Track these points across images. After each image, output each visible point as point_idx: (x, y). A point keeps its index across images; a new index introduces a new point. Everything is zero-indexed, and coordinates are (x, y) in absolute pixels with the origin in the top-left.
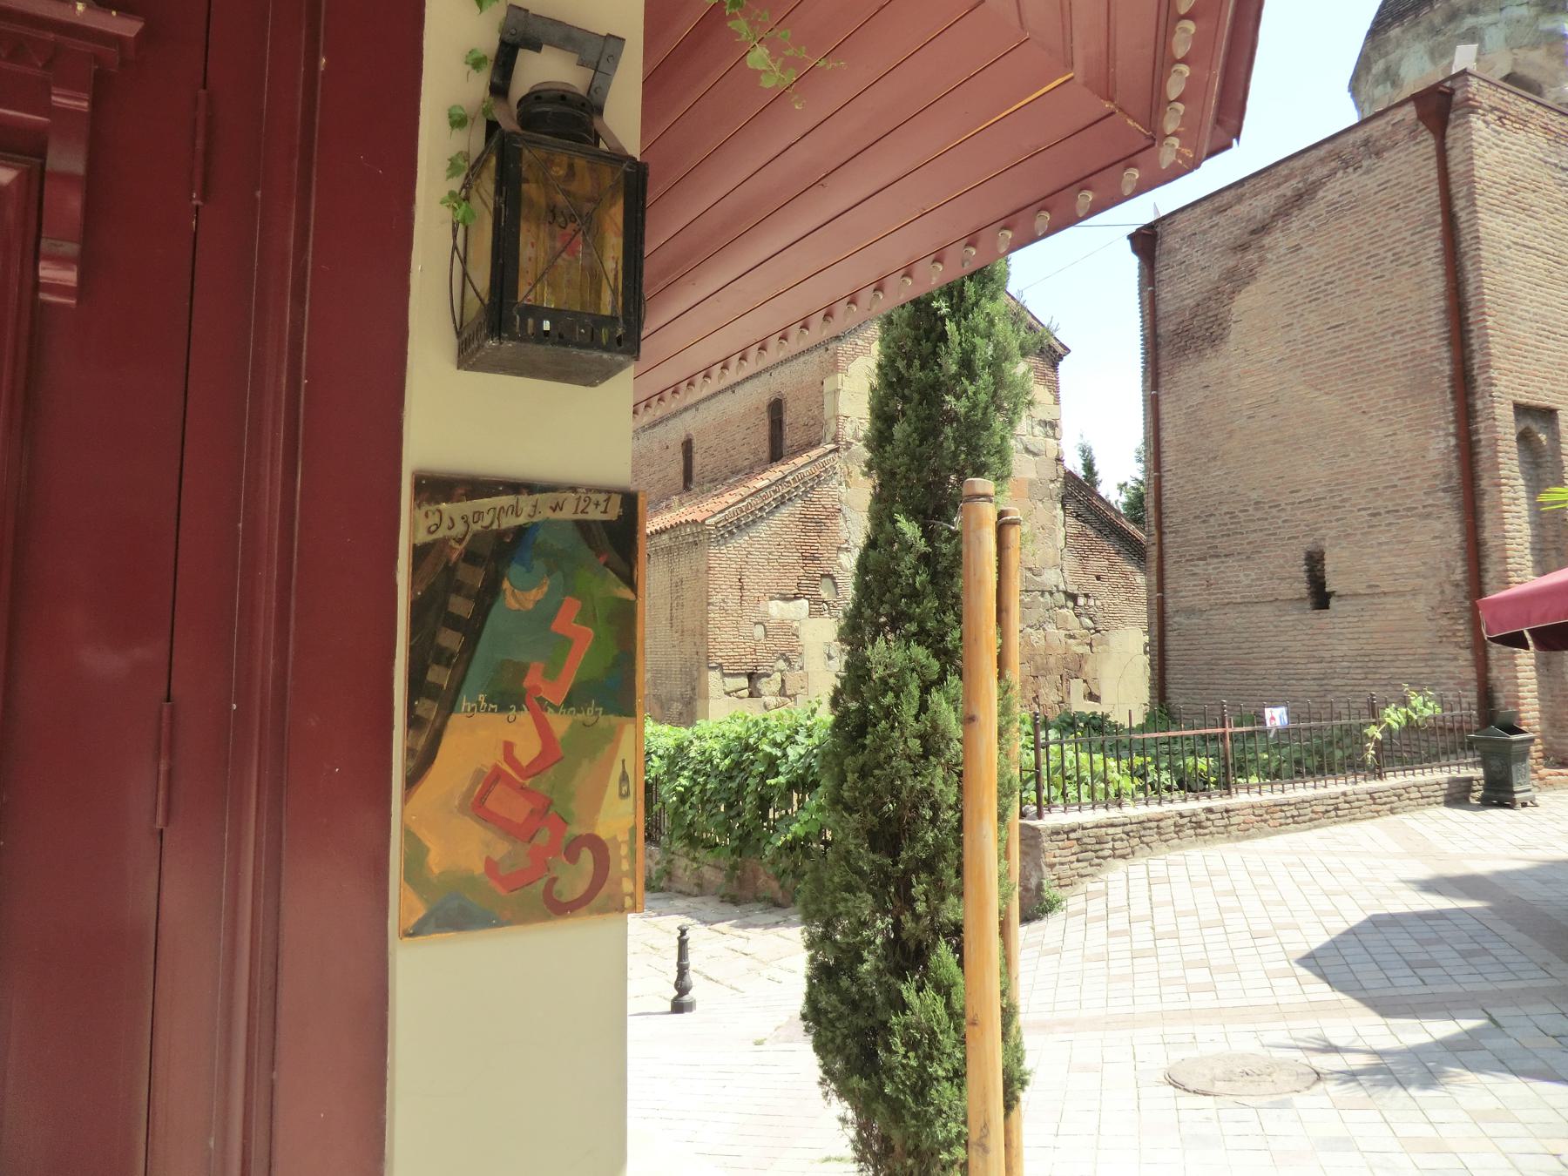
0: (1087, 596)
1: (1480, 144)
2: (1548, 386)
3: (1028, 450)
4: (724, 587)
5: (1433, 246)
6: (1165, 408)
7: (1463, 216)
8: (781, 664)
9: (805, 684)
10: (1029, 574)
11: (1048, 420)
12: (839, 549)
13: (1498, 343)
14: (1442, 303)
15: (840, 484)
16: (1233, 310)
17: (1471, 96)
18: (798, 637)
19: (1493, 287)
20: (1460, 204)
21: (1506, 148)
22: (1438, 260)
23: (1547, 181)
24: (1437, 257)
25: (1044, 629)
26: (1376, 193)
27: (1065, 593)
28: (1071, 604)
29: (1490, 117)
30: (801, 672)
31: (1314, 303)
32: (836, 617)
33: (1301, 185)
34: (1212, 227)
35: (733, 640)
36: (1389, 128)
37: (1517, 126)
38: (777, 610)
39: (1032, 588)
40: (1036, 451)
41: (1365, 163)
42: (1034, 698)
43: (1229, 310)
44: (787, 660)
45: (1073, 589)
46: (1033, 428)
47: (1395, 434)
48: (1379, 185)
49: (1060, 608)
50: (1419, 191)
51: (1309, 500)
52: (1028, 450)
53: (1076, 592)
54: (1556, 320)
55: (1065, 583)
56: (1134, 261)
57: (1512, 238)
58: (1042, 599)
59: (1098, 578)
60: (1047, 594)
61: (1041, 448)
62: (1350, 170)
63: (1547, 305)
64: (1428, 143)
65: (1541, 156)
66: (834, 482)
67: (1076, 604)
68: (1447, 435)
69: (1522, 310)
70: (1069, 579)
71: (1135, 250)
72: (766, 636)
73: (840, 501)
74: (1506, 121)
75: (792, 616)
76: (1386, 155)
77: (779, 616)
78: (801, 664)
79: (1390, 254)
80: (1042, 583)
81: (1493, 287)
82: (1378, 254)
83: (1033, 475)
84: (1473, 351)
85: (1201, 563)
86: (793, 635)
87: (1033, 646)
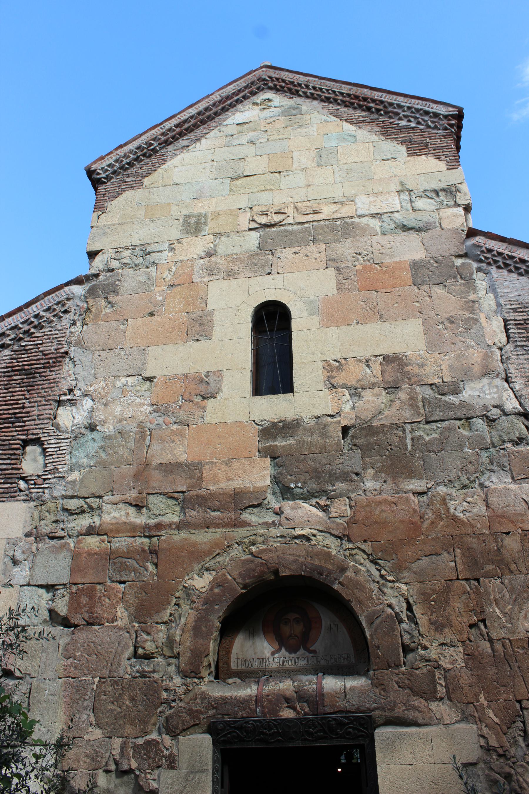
11: (438, 186)
12: (59, 403)
15: (74, 324)
25: (482, 485)
39: (438, 415)
40: (421, 225)
58: (466, 433)
73: (69, 343)
80: (463, 404)
83: (420, 255)
87: (455, 519)
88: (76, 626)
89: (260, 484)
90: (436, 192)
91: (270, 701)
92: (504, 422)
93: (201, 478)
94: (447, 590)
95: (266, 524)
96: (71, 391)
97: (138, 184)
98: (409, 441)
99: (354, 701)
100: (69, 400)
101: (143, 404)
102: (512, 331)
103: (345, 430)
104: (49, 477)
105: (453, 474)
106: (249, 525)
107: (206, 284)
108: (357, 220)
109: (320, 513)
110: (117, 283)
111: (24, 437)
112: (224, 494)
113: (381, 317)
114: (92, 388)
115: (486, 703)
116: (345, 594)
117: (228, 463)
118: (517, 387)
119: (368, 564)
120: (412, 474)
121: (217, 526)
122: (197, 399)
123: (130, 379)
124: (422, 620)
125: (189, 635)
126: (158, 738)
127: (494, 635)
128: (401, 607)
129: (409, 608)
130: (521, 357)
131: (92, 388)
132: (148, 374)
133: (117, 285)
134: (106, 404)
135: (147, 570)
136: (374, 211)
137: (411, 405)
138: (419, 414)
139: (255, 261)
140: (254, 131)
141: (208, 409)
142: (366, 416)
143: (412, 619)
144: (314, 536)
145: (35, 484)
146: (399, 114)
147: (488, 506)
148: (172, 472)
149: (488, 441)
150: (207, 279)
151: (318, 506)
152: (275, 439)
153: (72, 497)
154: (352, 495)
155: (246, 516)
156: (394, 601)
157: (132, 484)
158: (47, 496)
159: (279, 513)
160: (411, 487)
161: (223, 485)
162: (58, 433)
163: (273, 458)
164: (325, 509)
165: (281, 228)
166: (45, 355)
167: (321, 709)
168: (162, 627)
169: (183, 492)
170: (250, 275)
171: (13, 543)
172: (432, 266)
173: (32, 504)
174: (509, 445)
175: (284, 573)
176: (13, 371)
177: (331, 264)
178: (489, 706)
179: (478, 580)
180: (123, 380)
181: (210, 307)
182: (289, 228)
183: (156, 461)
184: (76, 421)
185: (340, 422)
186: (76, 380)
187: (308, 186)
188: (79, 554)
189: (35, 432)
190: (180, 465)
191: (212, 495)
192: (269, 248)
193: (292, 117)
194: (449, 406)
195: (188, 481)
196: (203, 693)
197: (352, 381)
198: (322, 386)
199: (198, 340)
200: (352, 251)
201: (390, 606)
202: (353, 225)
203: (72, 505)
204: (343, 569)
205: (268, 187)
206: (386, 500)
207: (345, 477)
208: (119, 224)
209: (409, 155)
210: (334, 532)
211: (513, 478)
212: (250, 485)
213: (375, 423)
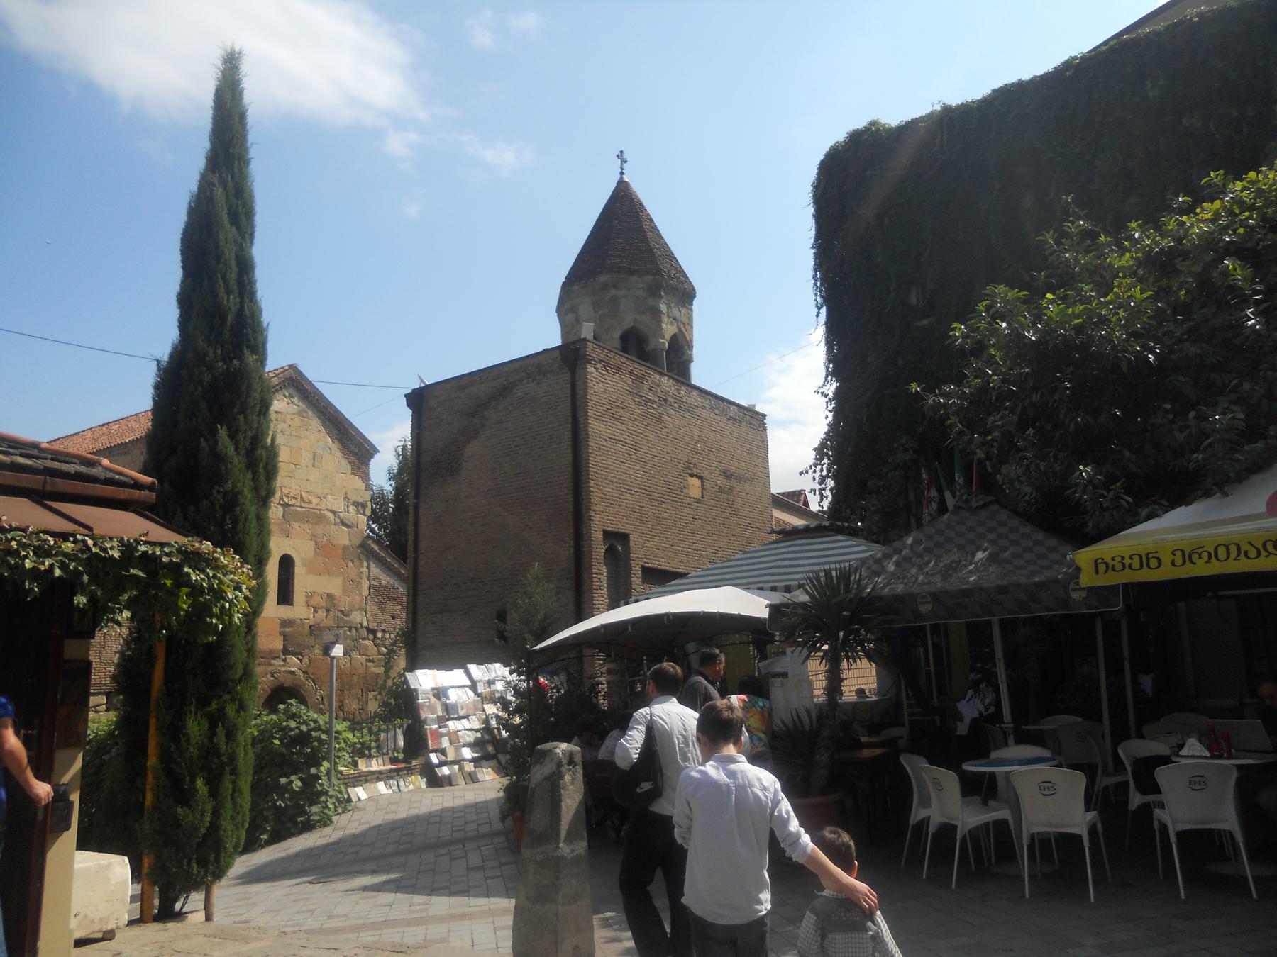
0: (384, 631)
1: (592, 381)
2: (625, 520)
5: (568, 435)
6: (422, 512)
7: (581, 419)
10: (340, 615)
11: (360, 501)
13: (596, 496)
14: (570, 469)
16: (465, 454)
17: (588, 353)
19: (594, 463)
20: (580, 413)
21: (607, 383)
22: (569, 443)
23: (630, 403)
24: (568, 441)
25: (350, 656)
26: (543, 397)
27: (367, 629)
28: (371, 637)
29: (598, 366)
31: (508, 458)
33: (505, 383)
34: (456, 398)
36: (551, 361)
37: (615, 371)
39: (342, 624)
40: (350, 524)
41: (538, 378)
42: (340, 707)
43: (462, 454)
45: (373, 626)
46: (348, 507)
47: (544, 543)
48: (544, 393)
49: (363, 640)
50: (562, 401)
51: (500, 580)
52: (343, 523)
53: (376, 628)
54: (631, 482)
56: (409, 412)
57: (608, 435)
58: (349, 633)
59: (393, 618)
60: (354, 630)
62: (530, 380)
63: (627, 474)
64: (567, 376)
65: (628, 388)
67: (375, 637)
68: (570, 546)
69: (611, 477)
70: (371, 618)
71: (409, 405)
74: (608, 368)
76: (548, 376)
79: (547, 435)
80: (350, 622)
81: (594, 463)
82: (541, 434)
83: (346, 542)
84: (583, 499)
85: (439, 615)
90: (358, 503)
103: (310, 627)
108: (326, 512)
109: (299, 662)
113: (329, 573)
116: (305, 694)
117: (267, 637)
118: (368, 616)
128: (320, 699)
129: (322, 700)
136: (334, 509)
140: (284, 422)
142: (319, 621)
143: (323, 704)
151: (298, 659)
155: (273, 661)
161: (265, 647)
165: (294, 508)
175: (285, 685)
177: (313, 538)
179: (343, 691)
182: (297, 508)
187: (308, 480)
194: (345, 621)
197: (315, 605)
198: (304, 605)
200: (323, 532)
201: (318, 699)
202: (325, 516)
205: (290, 475)
207: (308, 648)
209: (352, 474)
213: (321, 625)
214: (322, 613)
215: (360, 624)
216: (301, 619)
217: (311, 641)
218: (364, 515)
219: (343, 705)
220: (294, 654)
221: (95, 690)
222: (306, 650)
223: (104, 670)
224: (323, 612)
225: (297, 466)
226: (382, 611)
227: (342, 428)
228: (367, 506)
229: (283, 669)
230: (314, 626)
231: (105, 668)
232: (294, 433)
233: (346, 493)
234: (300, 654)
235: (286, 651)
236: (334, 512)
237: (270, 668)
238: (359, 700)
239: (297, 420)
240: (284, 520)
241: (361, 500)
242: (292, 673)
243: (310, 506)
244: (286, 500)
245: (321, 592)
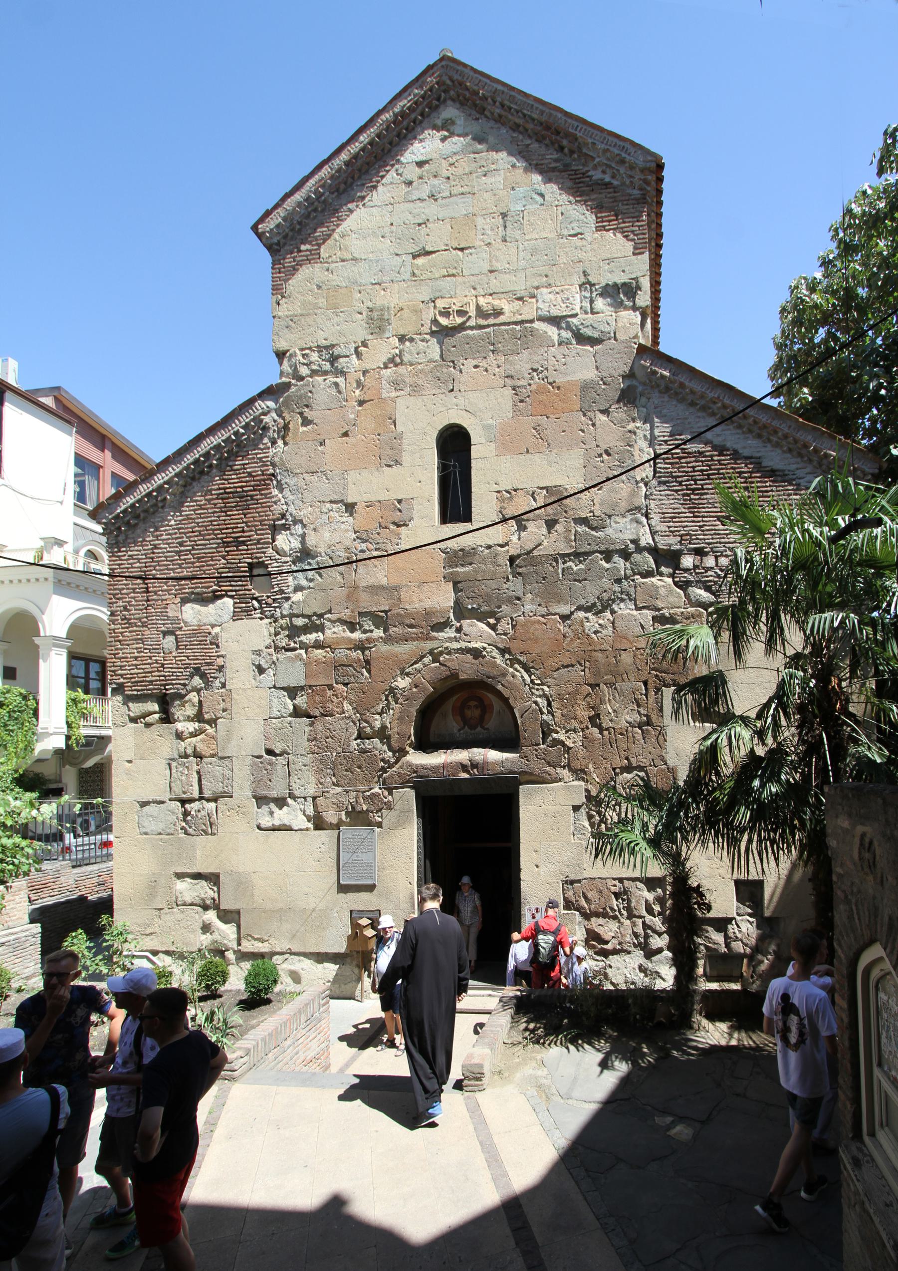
3: (581, 339)
4: (125, 591)
8: (197, 681)
9: (228, 705)
10: (581, 529)
18: (218, 646)
25: (613, 612)
27: (654, 551)
30: (223, 690)
32: (272, 616)
35: (136, 654)
38: (192, 613)
40: (596, 335)
42: (591, 718)
44: (203, 676)
45: (673, 542)
46: (592, 302)
52: (581, 339)
55: (653, 533)
58: (607, 565)
61: (607, 329)
66: (266, 440)
70: (662, 527)
72: (177, 648)
73: (274, 465)
75: (212, 620)
77: (195, 622)
78: (223, 680)
80: (607, 539)
83: (590, 374)
86: (212, 643)
88: (315, 717)
89: (445, 605)
91: (452, 768)
92: (637, 557)
93: (399, 599)
94: (577, 692)
95: (449, 638)
96: (283, 516)
97: (314, 257)
98: (560, 571)
99: (508, 766)
100: (284, 525)
101: (347, 531)
102: (659, 465)
103: (512, 560)
104: (277, 597)
105: (592, 600)
106: (437, 639)
107: (393, 400)
110: (310, 394)
111: (250, 561)
112: (417, 613)
114: (302, 513)
115: (592, 769)
119: (522, 671)
120: (559, 599)
121: (413, 639)
122: (392, 527)
123: (334, 506)
124: (558, 713)
125: (395, 723)
126: (380, 791)
127: (604, 725)
129: (549, 705)
130: (662, 493)
131: (302, 513)
132: (350, 500)
133: (310, 397)
134: (315, 529)
135: (362, 675)
137: (565, 538)
138: (571, 546)
139: (438, 374)
140: (435, 176)
141: (402, 536)
144: (484, 648)
145: (266, 603)
146: (593, 158)
147: (614, 628)
148: (377, 594)
149: (623, 573)
150: (394, 394)
151: (488, 624)
152: (457, 566)
153: (298, 616)
154: (514, 616)
156: (539, 700)
157: (345, 604)
158: (278, 614)
159: (459, 630)
160: (558, 610)
162: (277, 557)
163: (455, 584)
164: (493, 627)
166: (254, 476)
167: (486, 772)
168: (377, 717)
169: (386, 612)
170: (434, 392)
171: (258, 653)
172: (600, 388)
173: (267, 621)
174: (638, 577)
175: (462, 676)
176: (226, 493)
177: (509, 382)
178: (594, 772)
179: (598, 685)
180: (328, 505)
181: (400, 428)
182: (469, 332)
183: (363, 584)
184: (292, 545)
185: (508, 551)
186: (286, 503)
187: (491, 272)
188: (310, 663)
189: (258, 555)
190: (383, 588)
191: (410, 615)
192: (452, 358)
193: (477, 156)
195: (390, 602)
196: (408, 762)
199: (389, 466)
200: (528, 366)
201: (536, 703)
202: (532, 331)
203: (299, 622)
204: (504, 675)
206: (539, 621)
208: (302, 315)
209: (598, 229)
210: (499, 645)
211: (636, 605)
212: (437, 606)
214: (536, 530)
215: (633, 541)
216: (489, 547)
217: (515, 586)
218: (634, 308)
219: (598, 716)
220: (481, 617)
221: (138, 691)
222: (504, 607)
223: (149, 661)
224: (539, 527)
225: (467, 251)
226: (693, 508)
227: (565, 142)
228: (639, 288)
229: (456, 645)
230: (519, 556)
231: (150, 658)
232: (455, 191)
233: (585, 274)
234: (492, 614)
235: (460, 612)
236: (555, 321)
237: (429, 645)
238: (639, 706)
239: (464, 165)
240: (443, 360)
241: (620, 279)
242: (476, 653)
243: (502, 319)
244: (444, 321)
245: (531, 485)
